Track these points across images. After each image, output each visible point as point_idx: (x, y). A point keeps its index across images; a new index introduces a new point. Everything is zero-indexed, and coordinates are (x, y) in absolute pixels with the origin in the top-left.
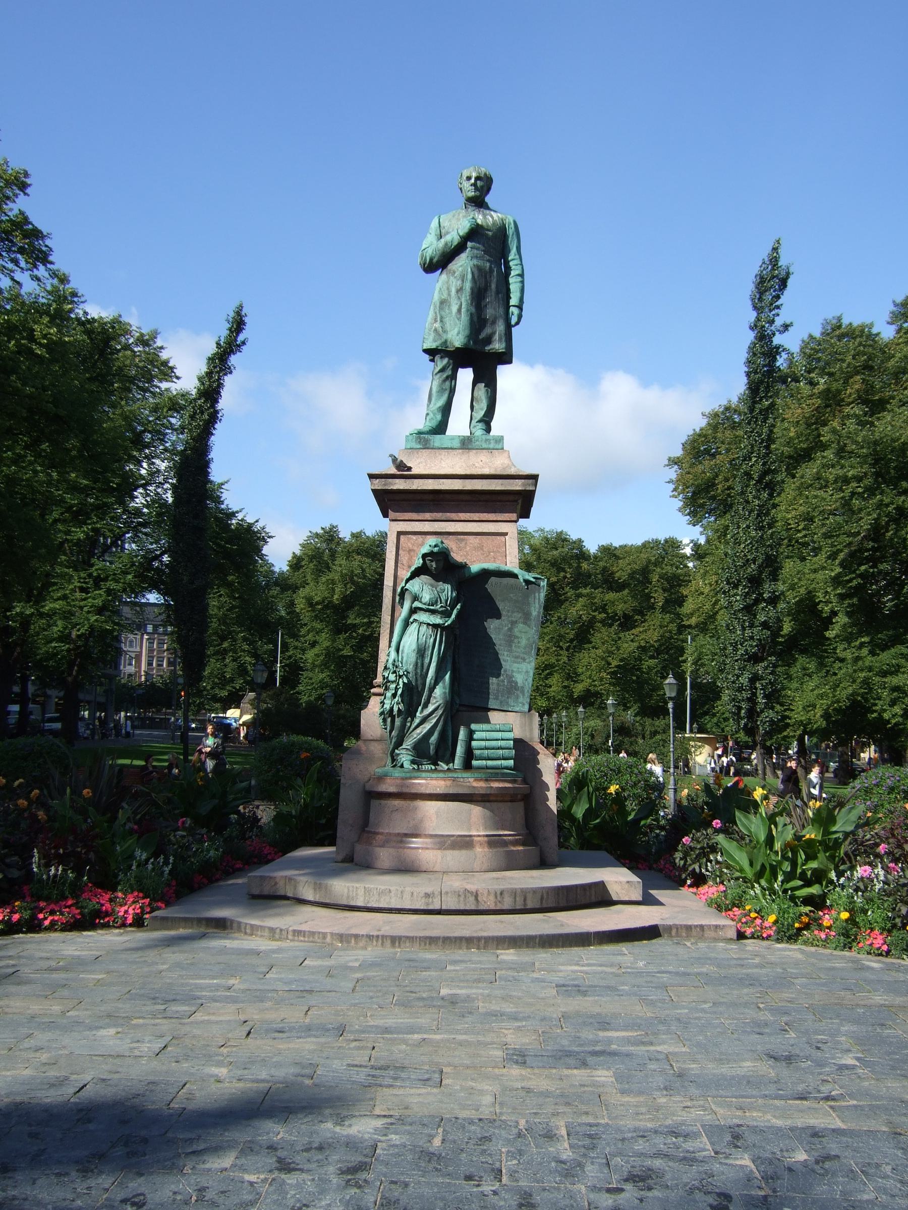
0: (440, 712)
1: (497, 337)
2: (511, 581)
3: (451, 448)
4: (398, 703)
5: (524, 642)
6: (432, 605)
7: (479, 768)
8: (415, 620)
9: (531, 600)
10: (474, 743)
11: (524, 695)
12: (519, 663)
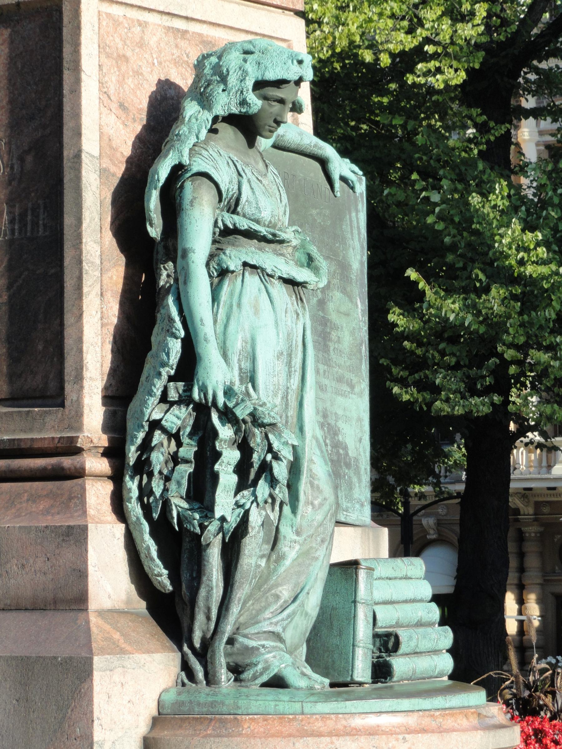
9: (346, 227)
12: (343, 395)
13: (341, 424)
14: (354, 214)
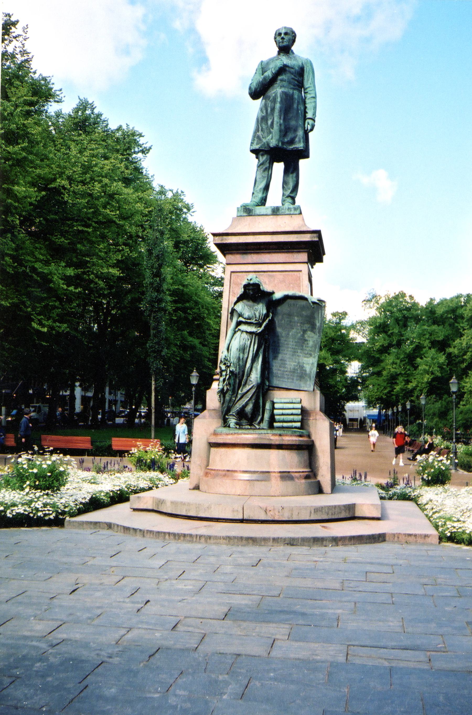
0: (253, 390)
1: (297, 139)
2: (303, 303)
3: (266, 215)
4: (226, 385)
5: (311, 343)
6: (250, 319)
7: (279, 428)
8: (239, 330)
10: (276, 412)
11: (310, 379)
12: (308, 357)
13: (305, 365)
14: (320, 311)
